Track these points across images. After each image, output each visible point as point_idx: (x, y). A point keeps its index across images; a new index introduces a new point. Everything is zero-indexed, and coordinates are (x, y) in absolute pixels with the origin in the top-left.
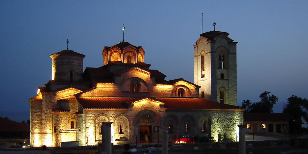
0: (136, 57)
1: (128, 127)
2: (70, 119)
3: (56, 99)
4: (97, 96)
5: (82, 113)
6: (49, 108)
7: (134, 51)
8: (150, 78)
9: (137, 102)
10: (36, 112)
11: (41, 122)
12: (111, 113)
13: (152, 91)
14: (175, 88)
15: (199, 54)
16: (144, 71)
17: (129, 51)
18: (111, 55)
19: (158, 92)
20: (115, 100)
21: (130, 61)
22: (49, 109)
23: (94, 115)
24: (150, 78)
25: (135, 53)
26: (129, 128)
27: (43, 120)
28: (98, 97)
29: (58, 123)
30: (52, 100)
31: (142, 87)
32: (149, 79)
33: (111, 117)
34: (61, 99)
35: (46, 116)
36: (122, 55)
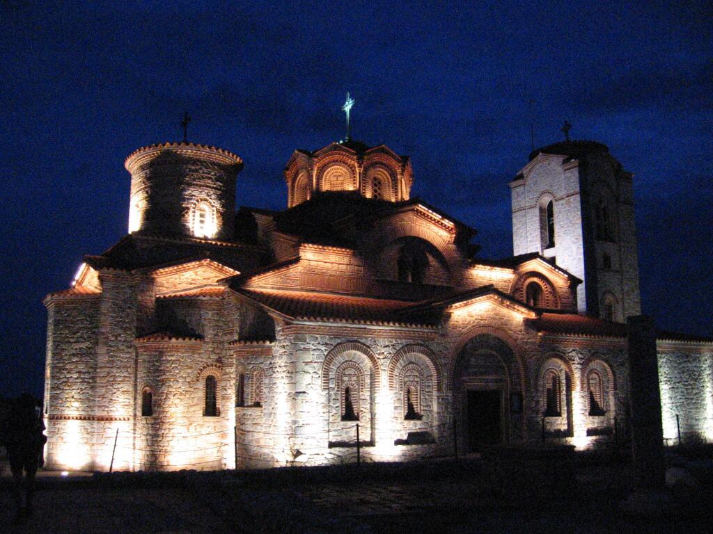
2: (204, 368)
3: (153, 294)
4: (299, 287)
5: (272, 339)
6: (122, 328)
9: (461, 306)
10: (72, 340)
11: (93, 378)
12: (382, 342)
15: (533, 203)
16: (438, 217)
17: (380, 164)
18: (322, 170)
22: (125, 329)
24: (454, 243)
25: (395, 171)
26: (438, 397)
27: (98, 370)
29: (163, 380)
30: (140, 298)
32: (452, 247)
33: (381, 357)
35: (111, 357)
36: (360, 173)
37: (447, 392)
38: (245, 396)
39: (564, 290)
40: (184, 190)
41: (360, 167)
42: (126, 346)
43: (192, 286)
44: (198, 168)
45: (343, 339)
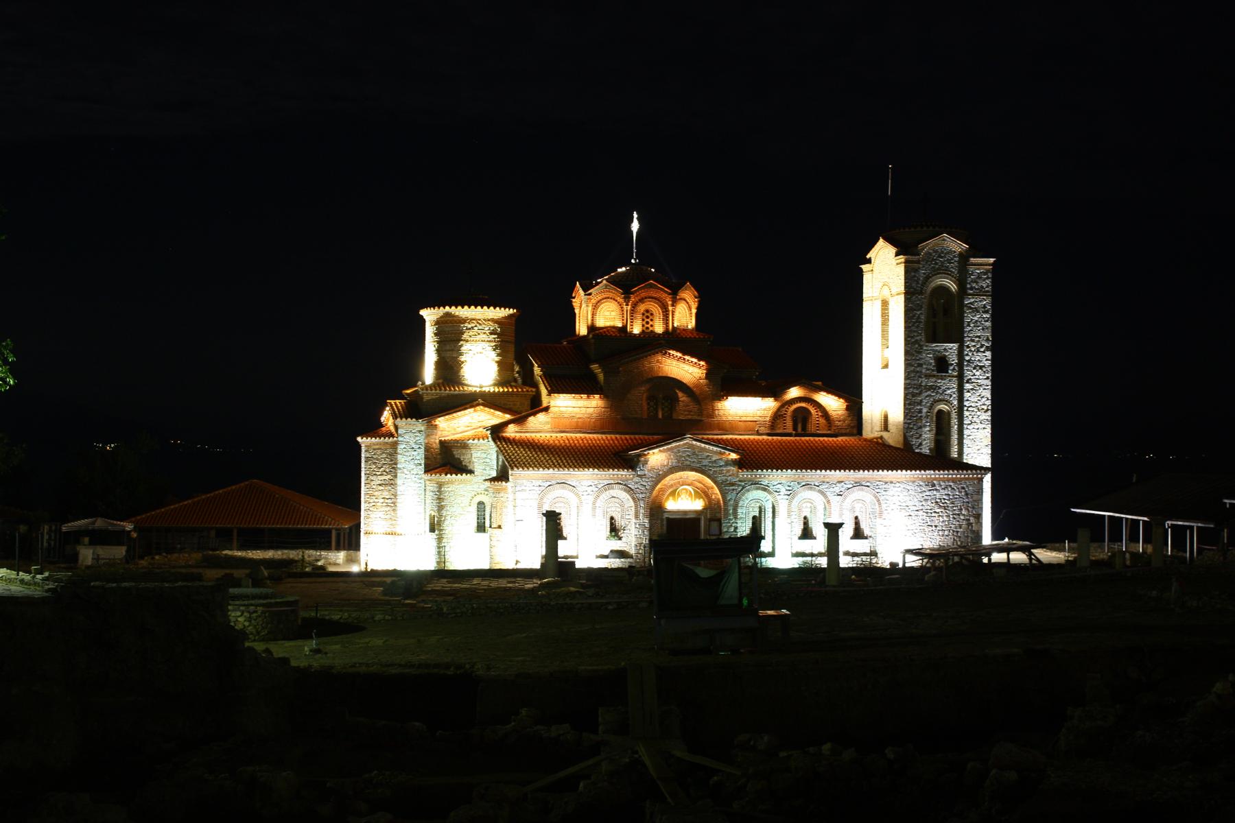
0: (668, 314)
1: (634, 520)
7: (664, 295)
8: (708, 376)
10: (377, 473)
13: (712, 415)
14: (782, 406)
17: (650, 297)
19: (730, 418)
20: (602, 442)
21: (652, 326)
23: (540, 486)
24: (706, 378)
26: (636, 524)
28: (554, 435)
31: (681, 404)
33: (585, 493)
34: (449, 438)
36: (627, 310)
37: (643, 519)
38: (492, 520)
39: (840, 413)
40: (462, 346)
41: (627, 305)
42: (418, 478)
43: (469, 428)
44: (473, 325)
45: (553, 482)
